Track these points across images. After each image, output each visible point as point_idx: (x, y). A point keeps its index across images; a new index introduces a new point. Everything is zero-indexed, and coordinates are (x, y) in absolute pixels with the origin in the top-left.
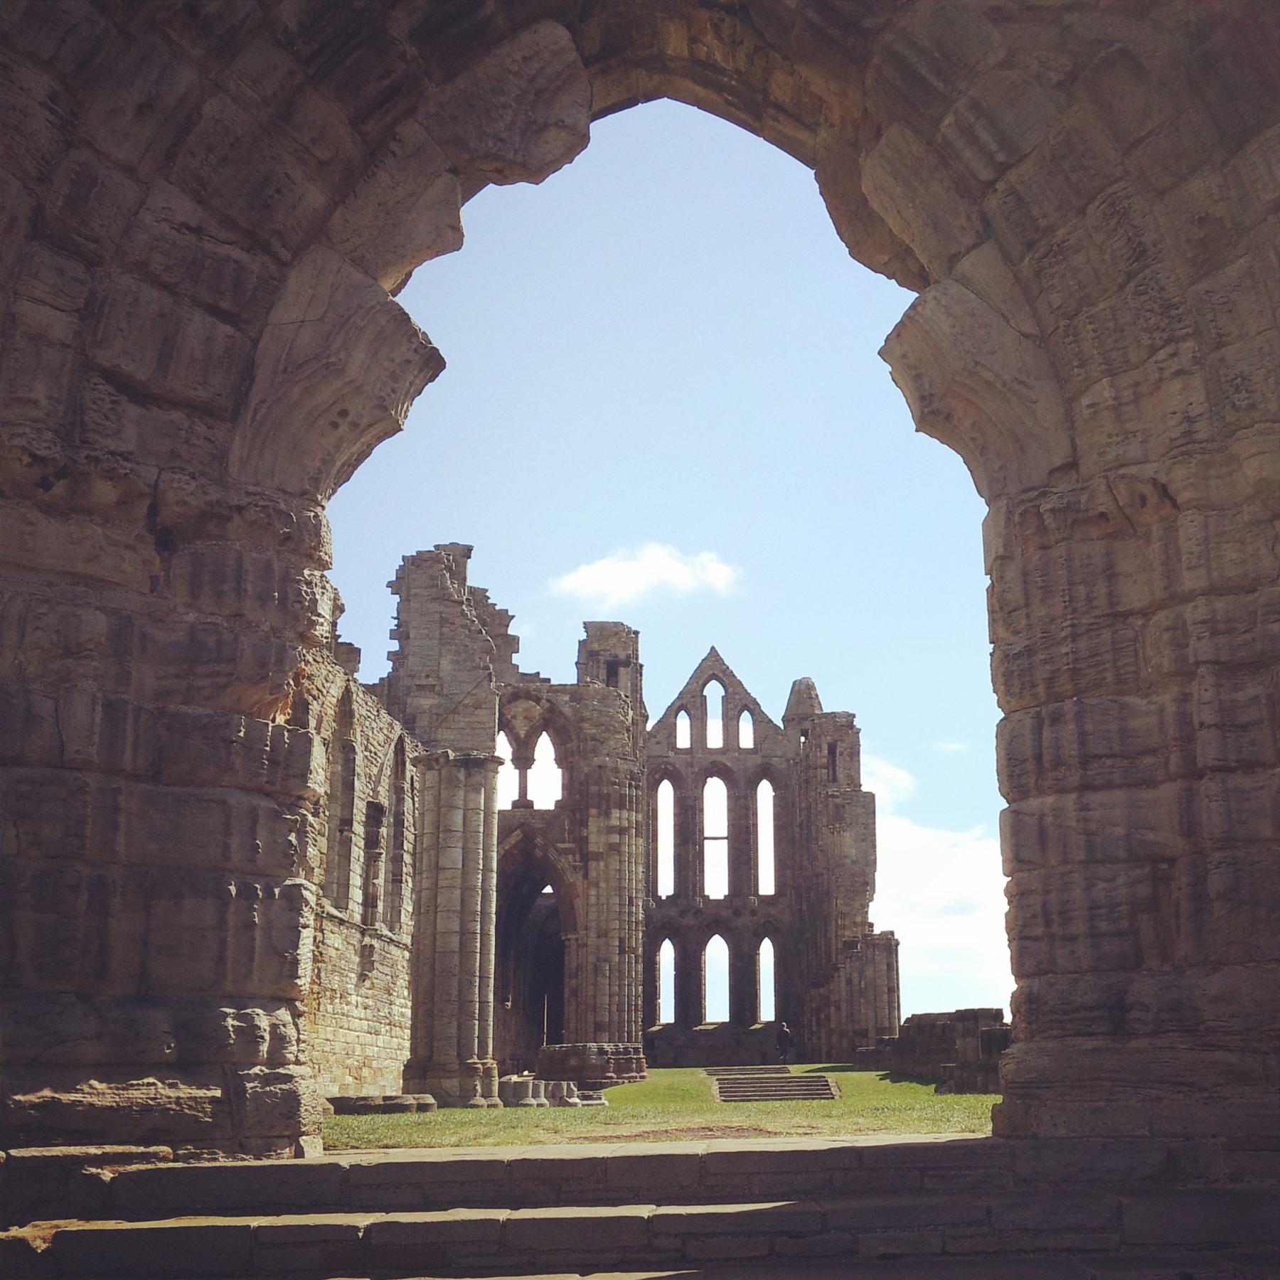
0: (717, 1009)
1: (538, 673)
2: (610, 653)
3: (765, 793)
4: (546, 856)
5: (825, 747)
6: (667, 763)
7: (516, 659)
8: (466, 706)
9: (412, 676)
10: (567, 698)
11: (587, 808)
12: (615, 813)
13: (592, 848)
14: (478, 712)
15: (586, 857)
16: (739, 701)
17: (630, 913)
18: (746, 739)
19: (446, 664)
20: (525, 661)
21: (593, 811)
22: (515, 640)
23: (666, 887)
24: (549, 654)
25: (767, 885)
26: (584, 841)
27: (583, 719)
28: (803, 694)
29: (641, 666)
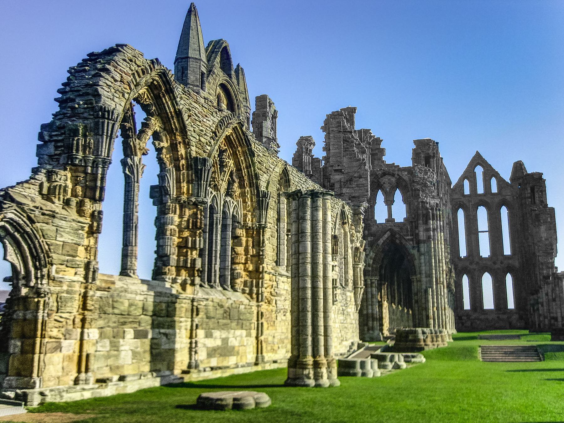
0: (489, 303)
2: (426, 152)
3: (504, 211)
4: (401, 243)
5: (529, 189)
6: (460, 201)
7: (384, 158)
8: (355, 177)
9: (332, 166)
10: (406, 173)
11: (418, 220)
14: (361, 180)
15: (418, 242)
16: (490, 173)
18: (494, 190)
19: (345, 160)
20: (388, 159)
21: (421, 222)
22: (383, 149)
23: (463, 253)
24: (399, 155)
25: (507, 251)
26: (417, 235)
27: (414, 182)
28: (519, 167)
29: (442, 158)
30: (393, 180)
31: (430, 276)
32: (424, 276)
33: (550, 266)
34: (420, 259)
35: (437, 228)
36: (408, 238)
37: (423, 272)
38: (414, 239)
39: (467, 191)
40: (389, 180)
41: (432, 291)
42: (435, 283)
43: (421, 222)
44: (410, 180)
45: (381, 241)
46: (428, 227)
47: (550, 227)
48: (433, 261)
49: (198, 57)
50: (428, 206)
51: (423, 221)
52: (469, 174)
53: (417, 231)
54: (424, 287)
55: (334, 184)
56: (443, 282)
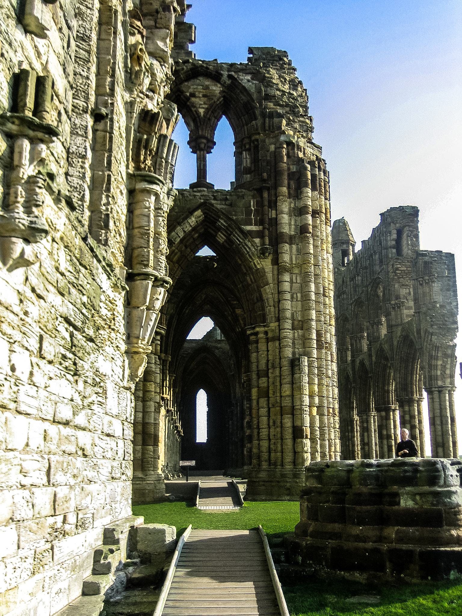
4: (229, 241)
5: (395, 232)
11: (277, 185)
26: (275, 223)
30: (217, 89)
32: (288, 325)
33: (449, 352)
34: (279, 282)
36: (248, 228)
37: (288, 314)
38: (267, 232)
40: (207, 88)
43: (285, 189)
44: (259, 91)
46: (301, 204)
47: (449, 285)
51: (289, 188)
53: (273, 214)
54: (288, 352)
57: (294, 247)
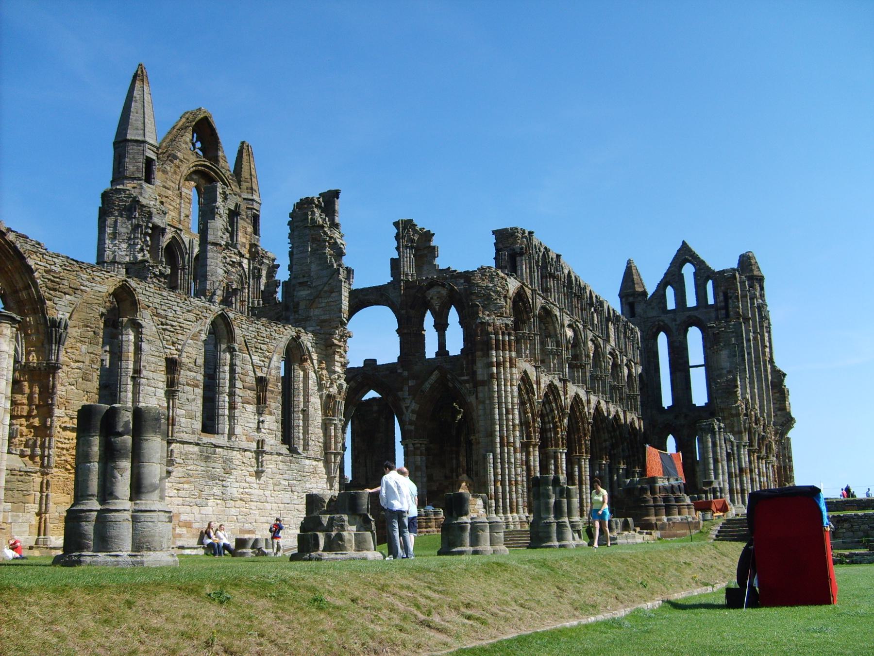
1: (449, 268)
5: (721, 294)
6: (659, 321)
7: (437, 261)
8: (326, 292)
10: (462, 281)
12: (494, 353)
13: (480, 377)
14: (334, 295)
16: (703, 273)
17: (507, 419)
20: (442, 262)
21: (479, 353)
22: (434, 247)
26: (474, 373)
29: (558, 256)
31: (492, 434)
35: (504, 361)
36: (463, 378)
39: (671, 305)
41: (494, 458)
42: (498, 445)
45: (427, 386)
48: (497, 411)
49: (140, 138)
50: (490, 329)
52: (673, 278)
55: (298, 304)
56: (514, 442)
57: (486, 388)
